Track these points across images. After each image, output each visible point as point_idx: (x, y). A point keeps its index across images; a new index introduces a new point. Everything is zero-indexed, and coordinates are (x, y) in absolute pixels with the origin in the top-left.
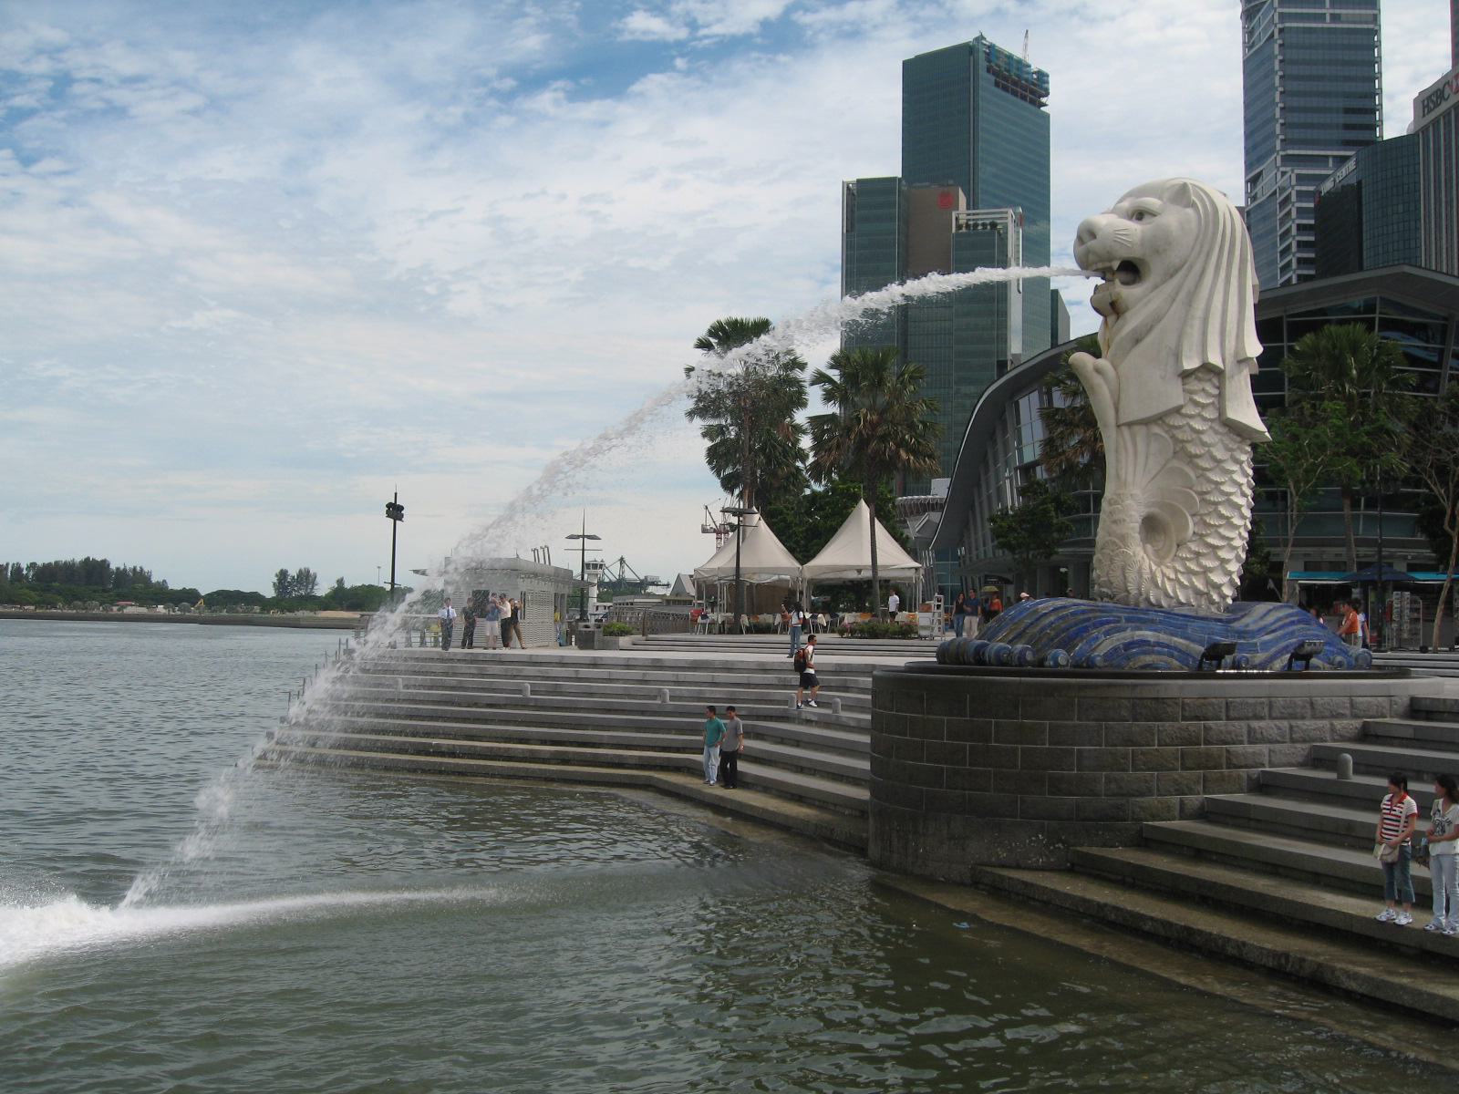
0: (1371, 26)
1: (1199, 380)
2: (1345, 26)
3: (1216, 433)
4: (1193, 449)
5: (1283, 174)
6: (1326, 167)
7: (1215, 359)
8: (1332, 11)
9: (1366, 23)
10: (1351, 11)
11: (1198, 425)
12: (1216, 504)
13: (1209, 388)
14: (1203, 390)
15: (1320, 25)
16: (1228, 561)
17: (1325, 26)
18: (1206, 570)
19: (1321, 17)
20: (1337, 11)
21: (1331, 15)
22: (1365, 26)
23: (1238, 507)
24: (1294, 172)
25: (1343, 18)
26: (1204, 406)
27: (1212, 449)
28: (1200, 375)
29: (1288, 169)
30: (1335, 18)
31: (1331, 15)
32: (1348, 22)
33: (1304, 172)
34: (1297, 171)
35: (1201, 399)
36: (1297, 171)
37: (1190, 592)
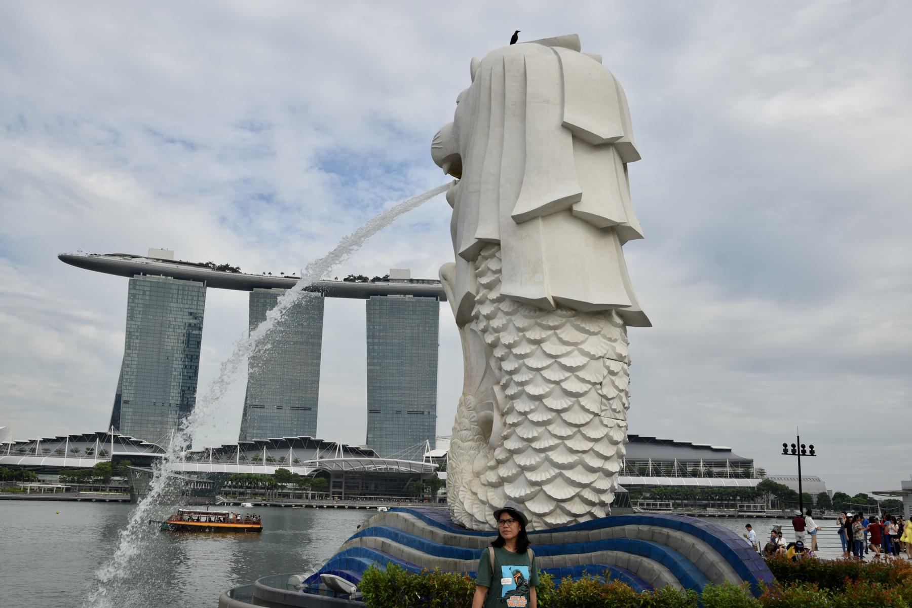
1: (486, 258)
3: (507, 314)
4: (489, 339)
7: (486, 231)
11: (485, 310)
12: (512, 398)
13: (493, 265)
14: (489, 269)
16: (531, 468)
18: (502, 481)
23: (538, 398)
26: (490, 287)
27: (501, 334)
28: (483, 254)
35: (484, 280)
37: (487, 508)
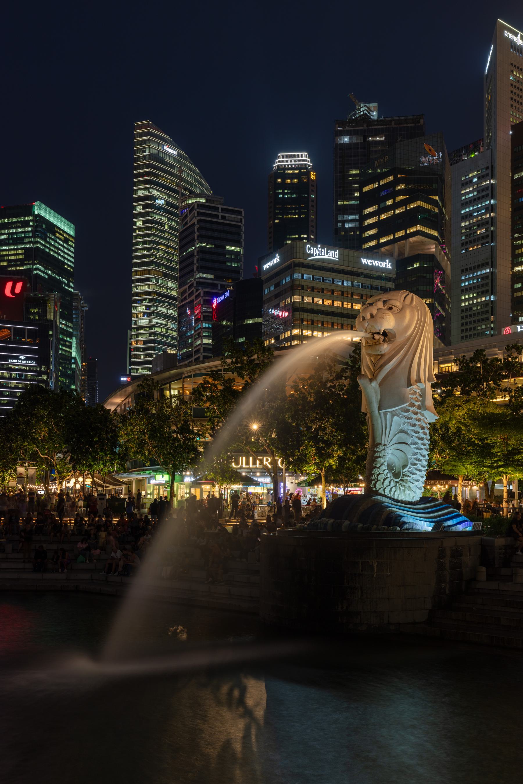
0: (239, 224)
2: (228, 222)
5: (197, 290)
6: (217, 289)
8: (222, 214)
9: (238, 222)
10: (230, 215)
15: (216, 220)
17: (219, 221)
19: (217, 217)
20: (224, 215)
21: (222, 216)
22: (236, 223)
24: (201, 290)
25: (227, 218)
29: (199, 288)
30: (223, 218)
31: (222, 216)
32: (228, 220)
33: (207, 290)
34: (204, 290)
36: (204, 290)
